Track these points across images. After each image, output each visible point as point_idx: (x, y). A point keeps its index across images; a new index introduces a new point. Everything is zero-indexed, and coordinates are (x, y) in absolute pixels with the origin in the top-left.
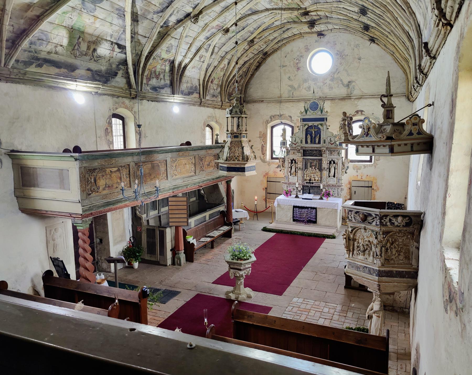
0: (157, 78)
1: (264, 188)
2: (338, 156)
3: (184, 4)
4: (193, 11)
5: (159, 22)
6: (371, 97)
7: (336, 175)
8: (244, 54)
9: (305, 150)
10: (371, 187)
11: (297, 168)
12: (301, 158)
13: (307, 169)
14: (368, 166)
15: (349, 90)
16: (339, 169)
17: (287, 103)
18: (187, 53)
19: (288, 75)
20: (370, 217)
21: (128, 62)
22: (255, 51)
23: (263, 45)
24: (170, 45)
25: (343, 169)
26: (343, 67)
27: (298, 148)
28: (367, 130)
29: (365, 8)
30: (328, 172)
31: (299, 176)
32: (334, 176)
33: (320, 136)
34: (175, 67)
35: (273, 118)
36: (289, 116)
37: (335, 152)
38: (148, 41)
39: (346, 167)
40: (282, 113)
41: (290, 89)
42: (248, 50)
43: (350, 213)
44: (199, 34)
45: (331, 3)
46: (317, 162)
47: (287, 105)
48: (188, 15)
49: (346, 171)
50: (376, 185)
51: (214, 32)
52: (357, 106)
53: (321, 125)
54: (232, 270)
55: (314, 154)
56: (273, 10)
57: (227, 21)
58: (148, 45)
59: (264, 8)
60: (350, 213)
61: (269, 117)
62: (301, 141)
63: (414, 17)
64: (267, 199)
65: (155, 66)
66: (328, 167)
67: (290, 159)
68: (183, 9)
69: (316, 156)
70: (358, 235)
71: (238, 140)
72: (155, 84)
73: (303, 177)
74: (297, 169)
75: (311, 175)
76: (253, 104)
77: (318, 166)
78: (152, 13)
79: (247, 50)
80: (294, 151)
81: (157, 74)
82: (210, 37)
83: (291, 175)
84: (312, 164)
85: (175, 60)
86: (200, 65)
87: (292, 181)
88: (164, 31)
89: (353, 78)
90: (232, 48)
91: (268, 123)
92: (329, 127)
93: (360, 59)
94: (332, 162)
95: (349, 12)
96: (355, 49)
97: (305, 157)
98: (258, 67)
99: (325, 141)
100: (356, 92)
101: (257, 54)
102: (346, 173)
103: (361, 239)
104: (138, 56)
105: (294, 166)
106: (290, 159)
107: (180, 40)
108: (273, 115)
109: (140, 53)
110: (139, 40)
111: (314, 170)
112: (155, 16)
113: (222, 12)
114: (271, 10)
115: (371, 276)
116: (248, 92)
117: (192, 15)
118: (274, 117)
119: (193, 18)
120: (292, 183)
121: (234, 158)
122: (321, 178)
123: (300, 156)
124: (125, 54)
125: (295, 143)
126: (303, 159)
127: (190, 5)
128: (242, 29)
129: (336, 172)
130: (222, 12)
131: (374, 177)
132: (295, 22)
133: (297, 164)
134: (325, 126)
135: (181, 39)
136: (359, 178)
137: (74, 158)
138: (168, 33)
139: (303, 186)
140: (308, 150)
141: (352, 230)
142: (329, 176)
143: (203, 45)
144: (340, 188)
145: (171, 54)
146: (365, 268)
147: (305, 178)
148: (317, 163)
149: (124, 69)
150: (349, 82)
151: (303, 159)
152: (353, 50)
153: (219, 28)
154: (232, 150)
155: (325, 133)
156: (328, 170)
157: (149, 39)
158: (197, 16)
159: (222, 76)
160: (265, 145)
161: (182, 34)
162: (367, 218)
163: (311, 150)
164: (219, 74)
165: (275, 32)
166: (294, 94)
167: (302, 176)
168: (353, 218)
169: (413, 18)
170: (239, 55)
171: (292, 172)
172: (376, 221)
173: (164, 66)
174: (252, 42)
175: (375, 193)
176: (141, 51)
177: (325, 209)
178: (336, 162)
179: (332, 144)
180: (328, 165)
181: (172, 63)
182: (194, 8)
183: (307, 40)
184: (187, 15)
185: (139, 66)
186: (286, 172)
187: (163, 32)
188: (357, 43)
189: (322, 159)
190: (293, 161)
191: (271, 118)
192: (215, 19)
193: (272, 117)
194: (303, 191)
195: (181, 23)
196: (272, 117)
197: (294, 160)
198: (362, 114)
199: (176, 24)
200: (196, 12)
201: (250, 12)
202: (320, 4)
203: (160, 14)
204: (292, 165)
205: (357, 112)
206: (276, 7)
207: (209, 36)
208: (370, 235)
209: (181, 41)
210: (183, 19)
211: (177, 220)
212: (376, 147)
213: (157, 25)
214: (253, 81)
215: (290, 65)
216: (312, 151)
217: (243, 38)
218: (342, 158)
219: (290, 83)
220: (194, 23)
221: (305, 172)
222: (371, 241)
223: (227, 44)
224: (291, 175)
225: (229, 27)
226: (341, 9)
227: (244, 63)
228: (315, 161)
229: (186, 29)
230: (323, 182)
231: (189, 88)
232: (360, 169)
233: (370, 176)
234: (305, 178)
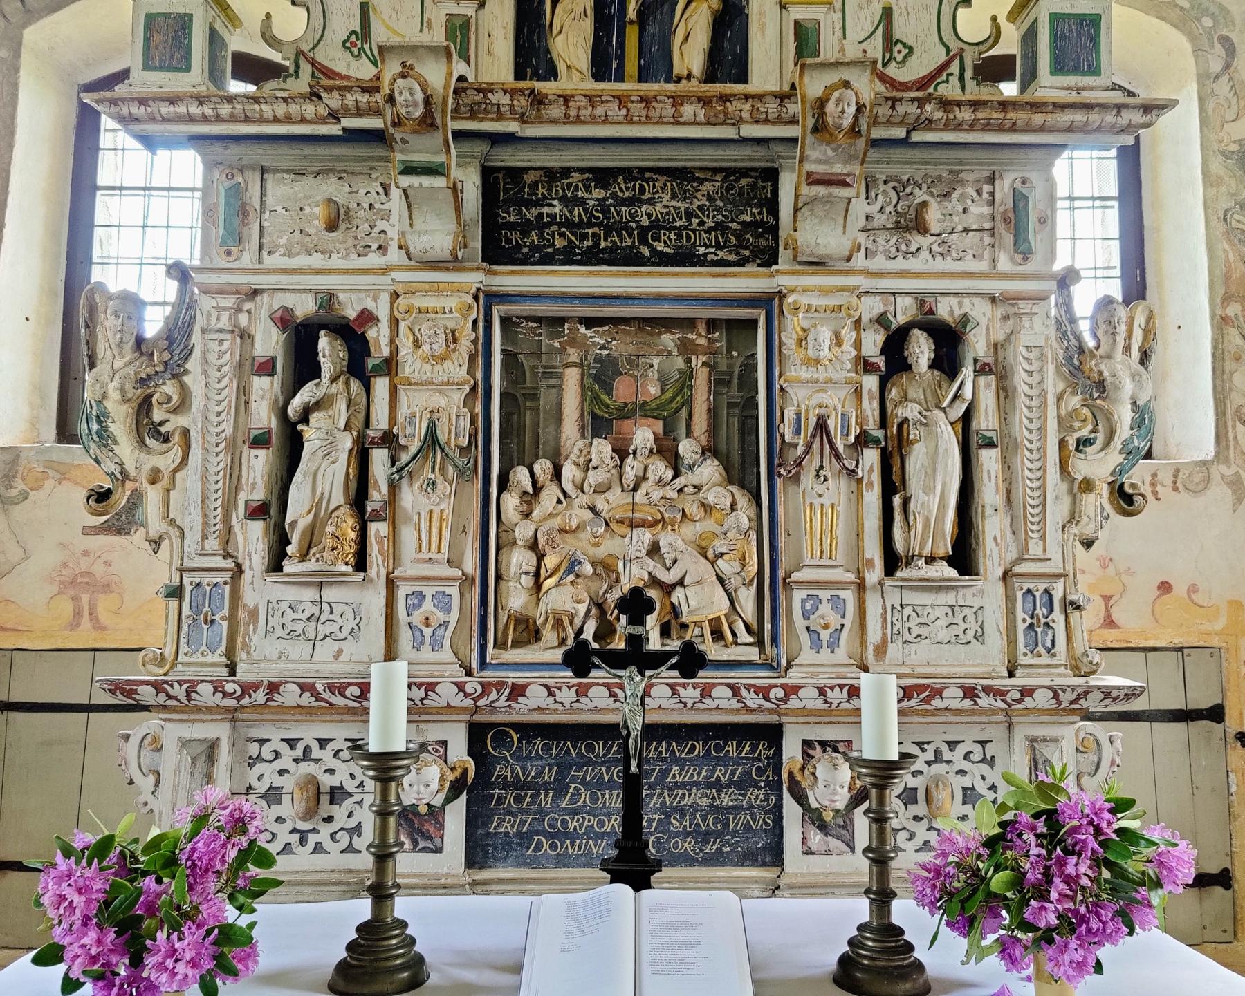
2: (1004, 264)
9: (515, 174)
11: (389, 440)
12: (455, 289)
13: (543, 467)
14: (1168, 481)
16: (1022, 426)
25: (1083, 443)
30: (873, 498)
31: (409, 568)
37: (954, 203)
39: (1124, 416)
46: (687, 349)
49: (1119, 471)
55: (656, 226)
66: (871, 409)
67: (266, 305)
69: (684, 258)
74: (379, 459)
75: (601, 552)
77: (713, 413)
80: (332, 188)
83: (276, 566)
84: (623, 390)
87: (298, 649)
94: (921, 350)
97: (511, 280)
102: (1125, 500)
105: (341, 412)
106: (266, 305)
111: (659, 468)
129: (989, 494)
133: (381, 386)
139: (477, 733)
140: (553, 175)
142: (892, 562)
147: (517, 599)
148: (687, 376)
151: (490, 298)
156: (871, 457)
163: (602, 176)
167: (470, 563)
178: (977, 345)
180: (871, 383)
186: (192, 520)
189: (769, 302)
190: (324, 343)
194: (474, 822)
204: (297, 402)
216: (623, 189)
218: (1066, 280)
221: (511, 502)
224: (276, 566)
228: (668, 340)
230: (807, 656)
233: (1193, 589)
234: (517, 599)
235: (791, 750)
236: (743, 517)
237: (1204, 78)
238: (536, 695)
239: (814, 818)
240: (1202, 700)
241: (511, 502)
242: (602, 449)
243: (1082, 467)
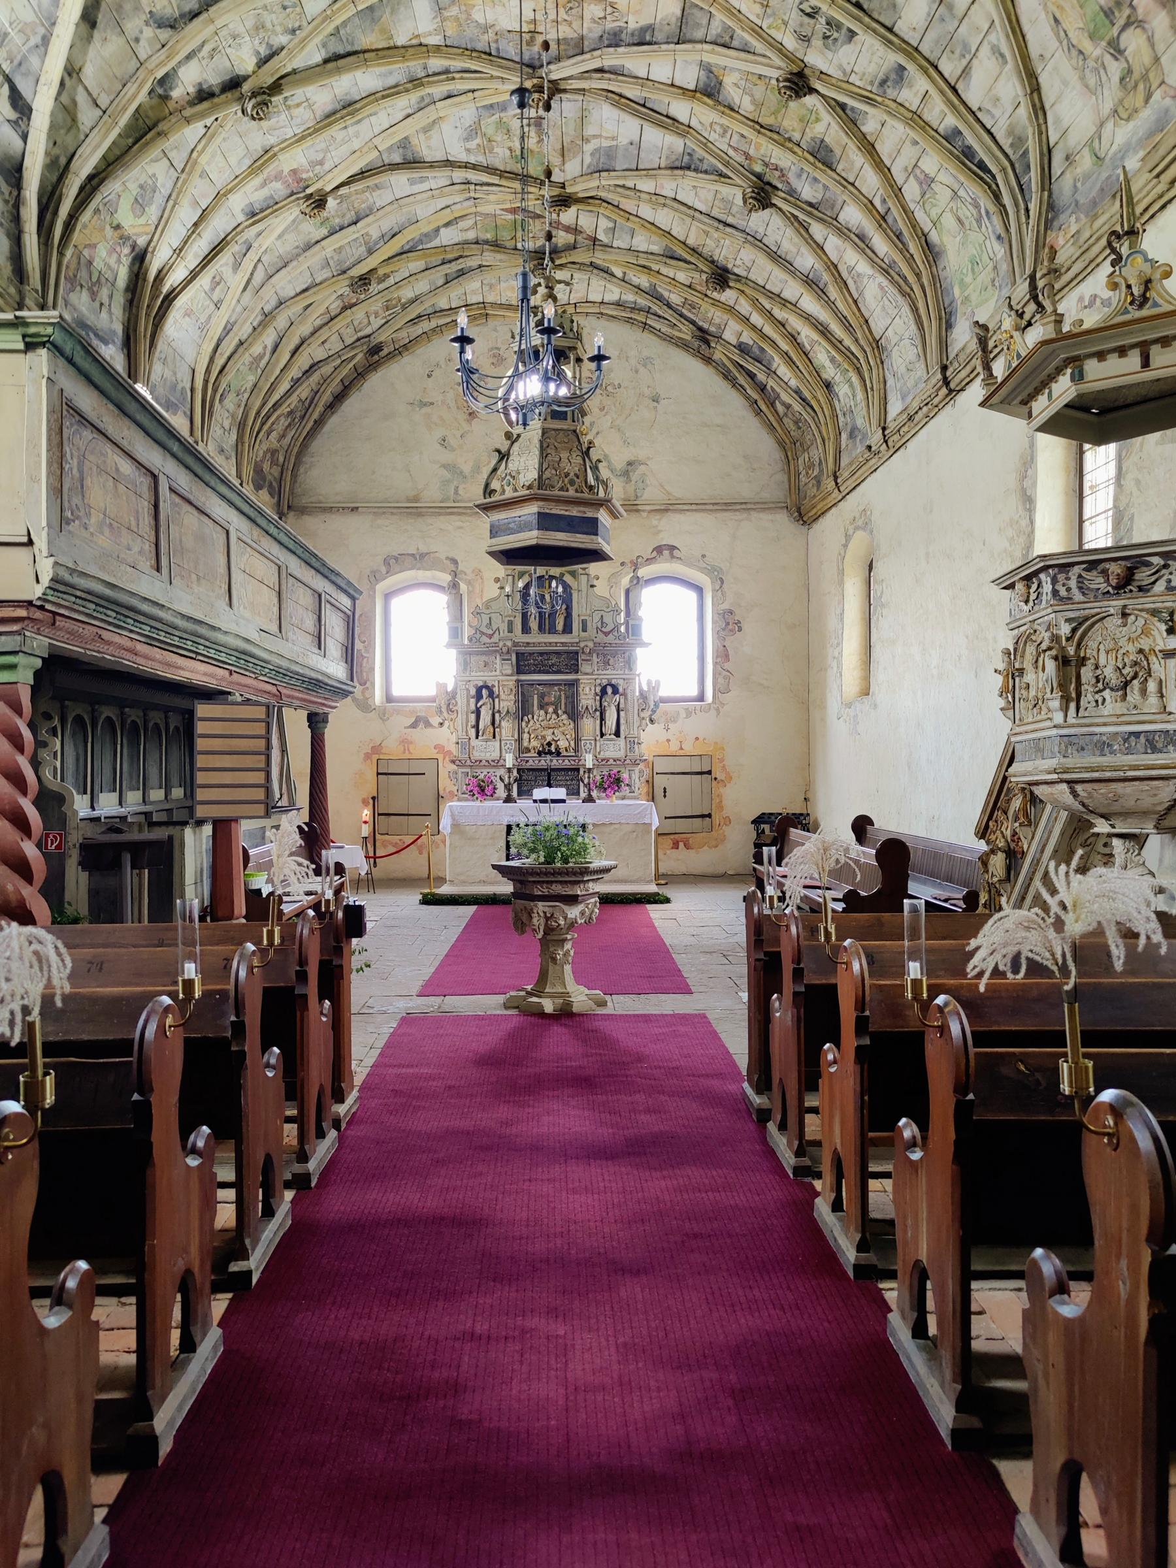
0: (93, 295)
1: (365, 796)
3: (241, 29)
4: (254, 72)
5: (150, 65)
6: (694, 507)
7: (622, 728)
8: (321, 331)
10: (709, 772)
11: (499, 712)
15: (631, 488)
16: (630, 707)
17: (441, 518)
18: (186, 243)
19: (439, 433)
20: (1145, 569)
21: (25, 174)
22: (350, 330)
23: (376, 315)
24: (150, 182)
26: (608, 417)
27: (505, 645)
28: (1142, 288)
29: (767, 187)
30: (598, 722)
32: (617, 734)
33: (569, 610)
34: (145, 280)
35: (393, 563)
36: (447, 558)
38: (101, 124)
40: (423, 549)
41: (448, 475)
42: (336, 316)
43: (1061, 577)
44: (238, 181)
45: (651, 172)
46: (560, 690)
47: (442, 522)
48: (233, 84)
50: (724, 766)
51: (277, 199)
52: (660, 531)
53: (573, 574)
54: (540, 904)
56: (466, 167)
57: (327, 166)
58: (97, 139)
59: (439, 156)
60: (1061, 577)
61: (380, 559)
62: (510, 623)
63: (1041, 121)
64: (378, 836)
65: (94, 241)
68: (229, 50)
69: (559, 672)
70: (1091, 644)
71: (565, 427)
72: (84, 309)
73: (520, 740)
74: (497, 715)
76: (322, 517)
78: (144, 17)
79: (332, 319)
80: (484, 658)
81: (94, 279)
82: (262, 211)
83: (477, 737)
84: (546, 699)
85: (150, 249)
86: (208, 312)
88: (150, 113)
89: (641, 454)
90: (298, 290)
91: (377, 581)
92: (595, 582)
93: (656, 400)
94: (609, 690)
95: (691, 212)
96: (642, 369)
97: (523, 677)
98: (339, 398)
99: (584, 623)
100: (651, 494)
101: (352, 346)
102: (652, 721)
103: (1107, 653)
104: (58, 170)
107: (183, 176)
108: (395, 554)
109: (63, 161)
110: (75, 103)
111: (554, 716)
112: (148, 32)
113: (330, 118)
114: (460, 167)
115: (1160, 755)
116: (300, 479)
117: (246, 87)
118: (396, 559)
119: (254, 95)
120: (484, 763)
121: (566, 480)
122: (577, 740)
123: (509, 672)
124: (25, 137)
125: (490, 632)
126: (518, 681)
127: (257, 42)
128: (350, 221)
129: (622, 721)
130: (328, 116)
131: (716, 743)
132: (496, 245)
134: (584, 579)
135: (189, 174)
136: (674, 748)
137: (24, 336)
138: (161, 127)
139: (519, 770)
140: (531, 654)
141: (1074, 630)
142: (602, 735)
143: (237, 235)
144: (637, 769)
145: (142, 221)
146: (1133, 738)
147: (525, 744)
149: (7, 197)
150: (630, 464)
152: (637, 372)
153: (295, 187)
154: (549, 457)
155: (583, 601)
157: (106, 117)
158: (264, 93)
159: (249, 390)
160: (367, 651)
161: (195, 154)
162: (1133, 574)
163: (541, 654)
164: (242, 376)
165: (427, 272)
166: (460, 492)
167: (516, 736)
168: (1075, 591)
169: (1039, 125)
170: (305, 329)
171: (481, 726)
172: (1165, 578)
173: (115, 256)
174: (365, 284)
175: (722, 790)
176: (69, 155)
177: (612, 827)
178: (621, 690)
179: (606, 634)
181: (140, 258)
182: (263, 62)
183: (495, 330)
184: (231, 80)
185: (56, 213)
187: (147, 117)
188: (646, 353)
189: (577, 680)
191: (386, 562)
192: (303, 138)
193: (392, 561)
195: (205, 105)
196: (392, 561)
197: (487, 687)
198: (672, 557)
199: (192, 104)
200: (267, 78)
201: (397, 158)
202: (612, 174)
203: (164, 34)
205: (659, 550)
206: (479, 159)
207: (257, 207)
208: (1139, 631)
209: (185, 182)
210: (217, 90)
211: (226, 794)
212: (1155, 350)
213: (141, 74)
214: (316, 445)
215: (443, 402)
217: (340, 262)
219: (447, 457)
220: (254, 119)
222: (1147, 648)
223: (294, 263)
224: (477, 737)
225: (328, 188)
226: (668, 202)
227: (311, 367)
228: (556, 688)
229: (213, 136)
231: (168, 383)
232: (675, 721)
235: (581, 772)
236: (572, 725)
237: (714, 591)
238: (531, 762)
239: (585, 785)
240: (706, 769)
241: (524, 724)
242: (542, 712)
243: (642, 715)
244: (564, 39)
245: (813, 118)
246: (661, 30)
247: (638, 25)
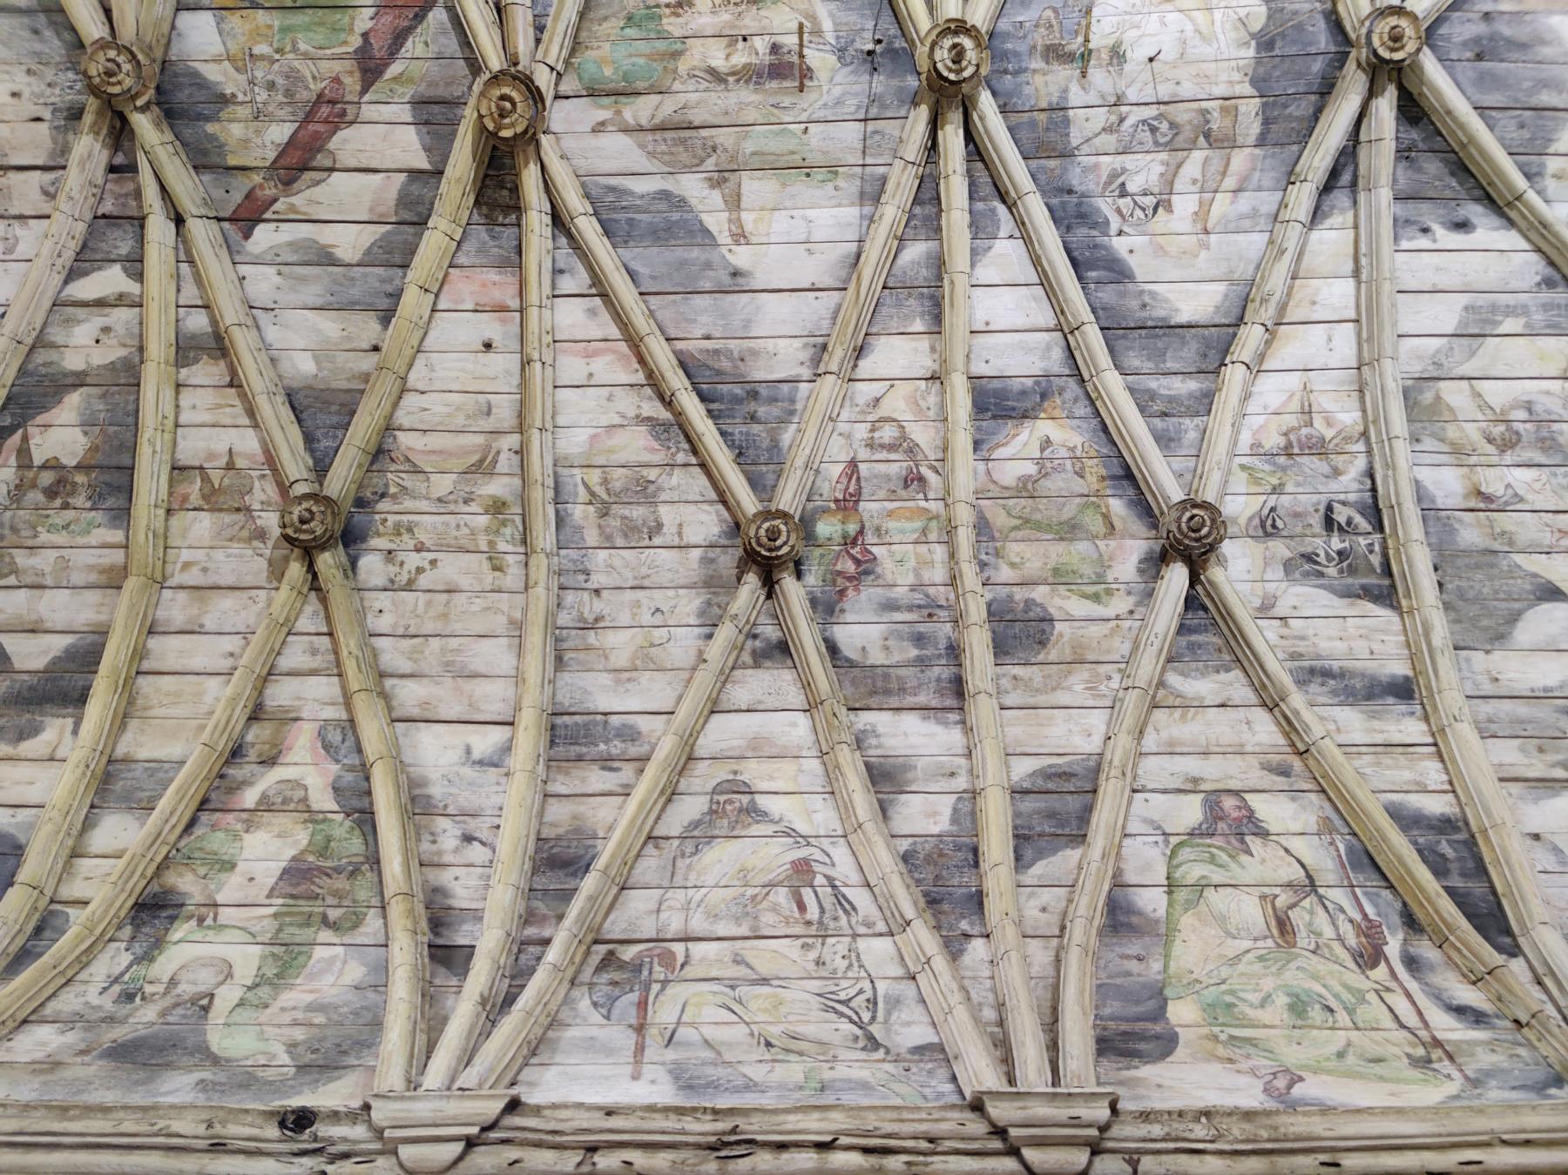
244: (1067, 122)
245: (1090, 589)
246: (1123, 295)
247: (1124, 254)
